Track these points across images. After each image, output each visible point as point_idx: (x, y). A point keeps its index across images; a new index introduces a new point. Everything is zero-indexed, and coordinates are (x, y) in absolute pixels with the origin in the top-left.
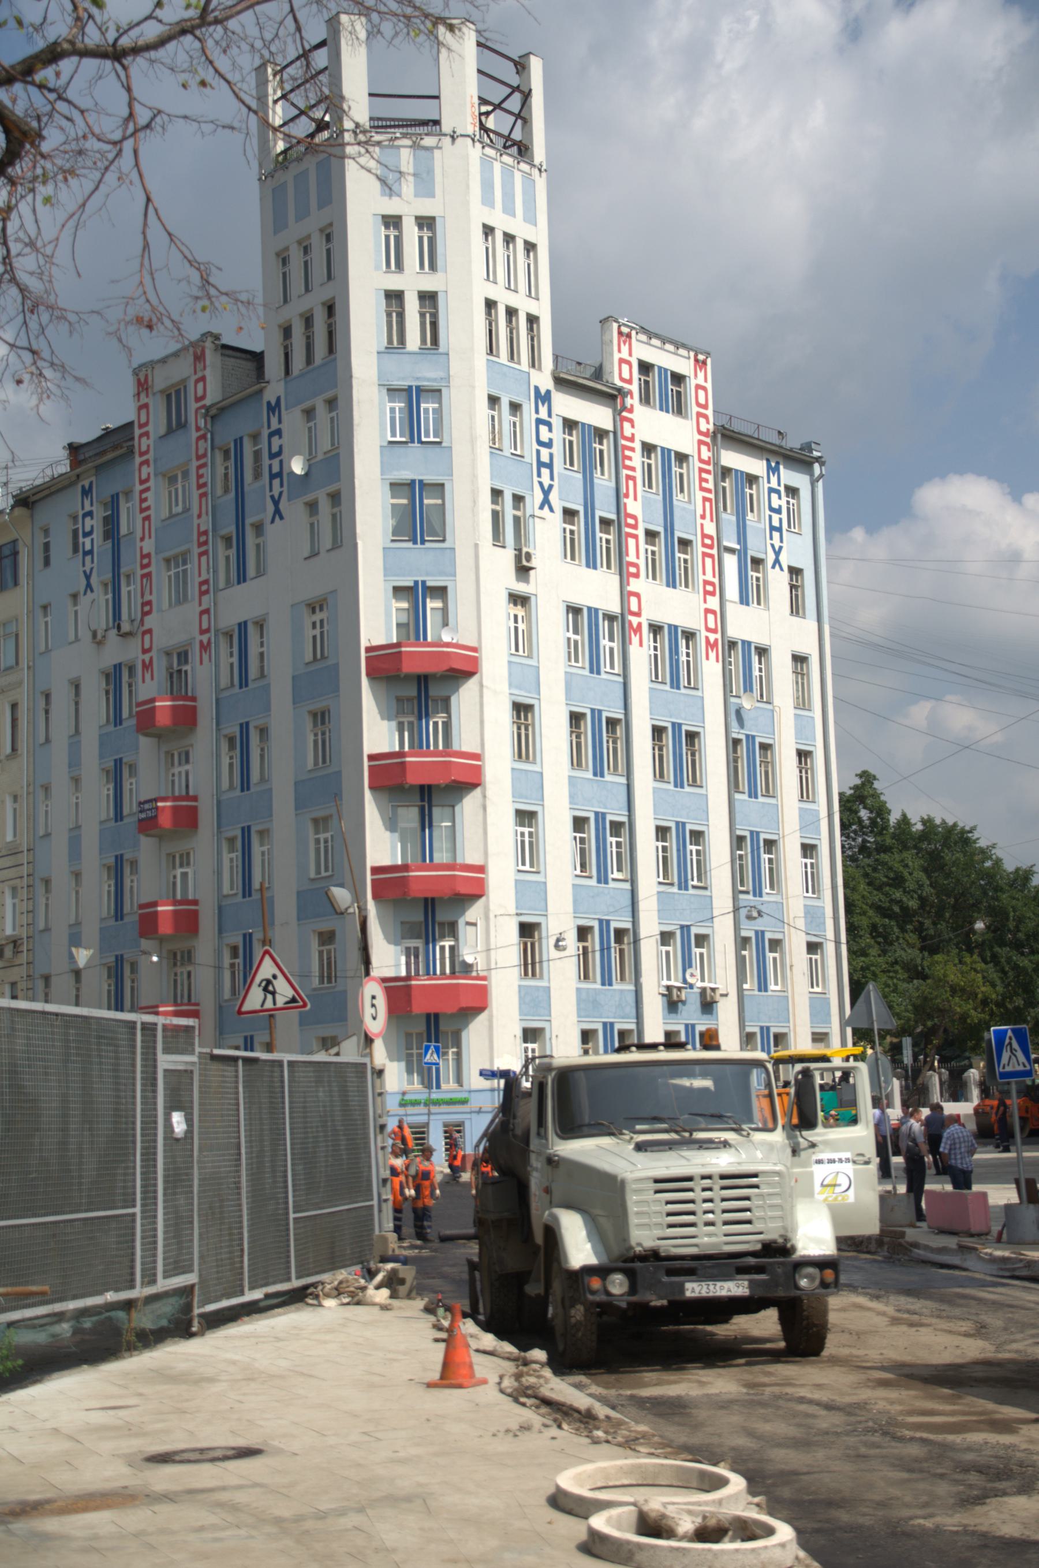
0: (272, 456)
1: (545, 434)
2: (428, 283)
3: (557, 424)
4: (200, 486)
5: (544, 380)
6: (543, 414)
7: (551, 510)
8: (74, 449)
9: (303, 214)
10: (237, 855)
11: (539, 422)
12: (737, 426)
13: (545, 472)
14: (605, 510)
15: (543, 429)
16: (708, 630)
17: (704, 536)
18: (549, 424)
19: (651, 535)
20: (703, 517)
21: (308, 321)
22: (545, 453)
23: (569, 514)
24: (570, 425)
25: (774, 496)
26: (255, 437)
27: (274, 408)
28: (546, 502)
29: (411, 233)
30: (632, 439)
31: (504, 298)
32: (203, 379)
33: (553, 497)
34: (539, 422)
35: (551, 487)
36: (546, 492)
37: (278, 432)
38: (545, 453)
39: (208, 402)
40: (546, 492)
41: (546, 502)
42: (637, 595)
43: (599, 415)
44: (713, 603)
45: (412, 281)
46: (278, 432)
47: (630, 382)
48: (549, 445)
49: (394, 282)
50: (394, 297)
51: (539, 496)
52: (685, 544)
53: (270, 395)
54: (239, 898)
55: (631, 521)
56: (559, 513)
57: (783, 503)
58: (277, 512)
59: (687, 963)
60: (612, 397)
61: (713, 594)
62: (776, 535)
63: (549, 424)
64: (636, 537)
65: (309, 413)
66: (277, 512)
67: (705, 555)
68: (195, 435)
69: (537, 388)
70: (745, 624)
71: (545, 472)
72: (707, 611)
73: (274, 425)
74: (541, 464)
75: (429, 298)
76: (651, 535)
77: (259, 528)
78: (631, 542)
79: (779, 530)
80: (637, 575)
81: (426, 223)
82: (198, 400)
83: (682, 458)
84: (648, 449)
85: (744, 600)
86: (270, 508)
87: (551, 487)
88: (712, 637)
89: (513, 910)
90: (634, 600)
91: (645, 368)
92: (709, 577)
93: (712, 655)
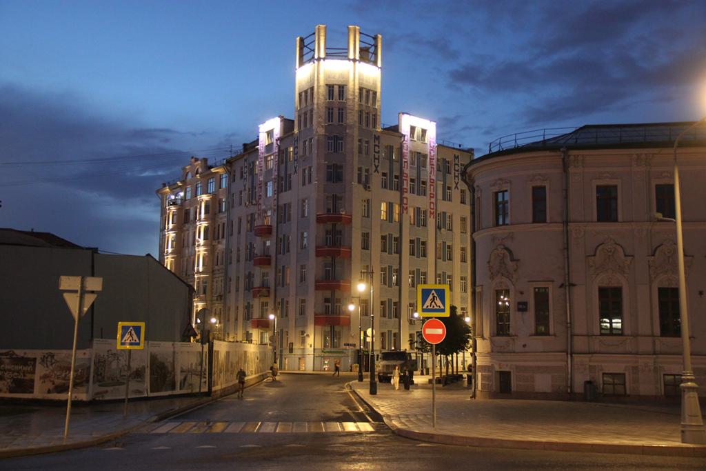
6: (377, 143)
7: (378, 172)
8: (245, 145)
14: (396, 173)
16: (431, 209)
17: (431, 179)
19: (412, 180)
20: (431, 173)
22: (377, 155)
25: (456, 166)
28: (376, 170)
34: (375, 146)
35: (378, 166)
36: (377, 167)
38: (377, 155)
40: (377, 167)
41: (376, 170)
42: (407, 198)
44: (433, 200)
51: (374, 169)
52: (424, 183)
55: (405, 175)
56: (380, 174)
61: (433, 197)
62: (456, 178)
63: (379, 147)
67: (430, 185)
69: (375, 136)
70: (443, 206)
71: (377, 161)
72: (431, 203)
74: (375, 159)
76: (412, 180)
78: (405, 182)
80: (406, 192)
85: (444, 199)
87: (378, 166)
88: (432, 211)
90: (405, 200)
92: (432, 192)
93: (432, 217)
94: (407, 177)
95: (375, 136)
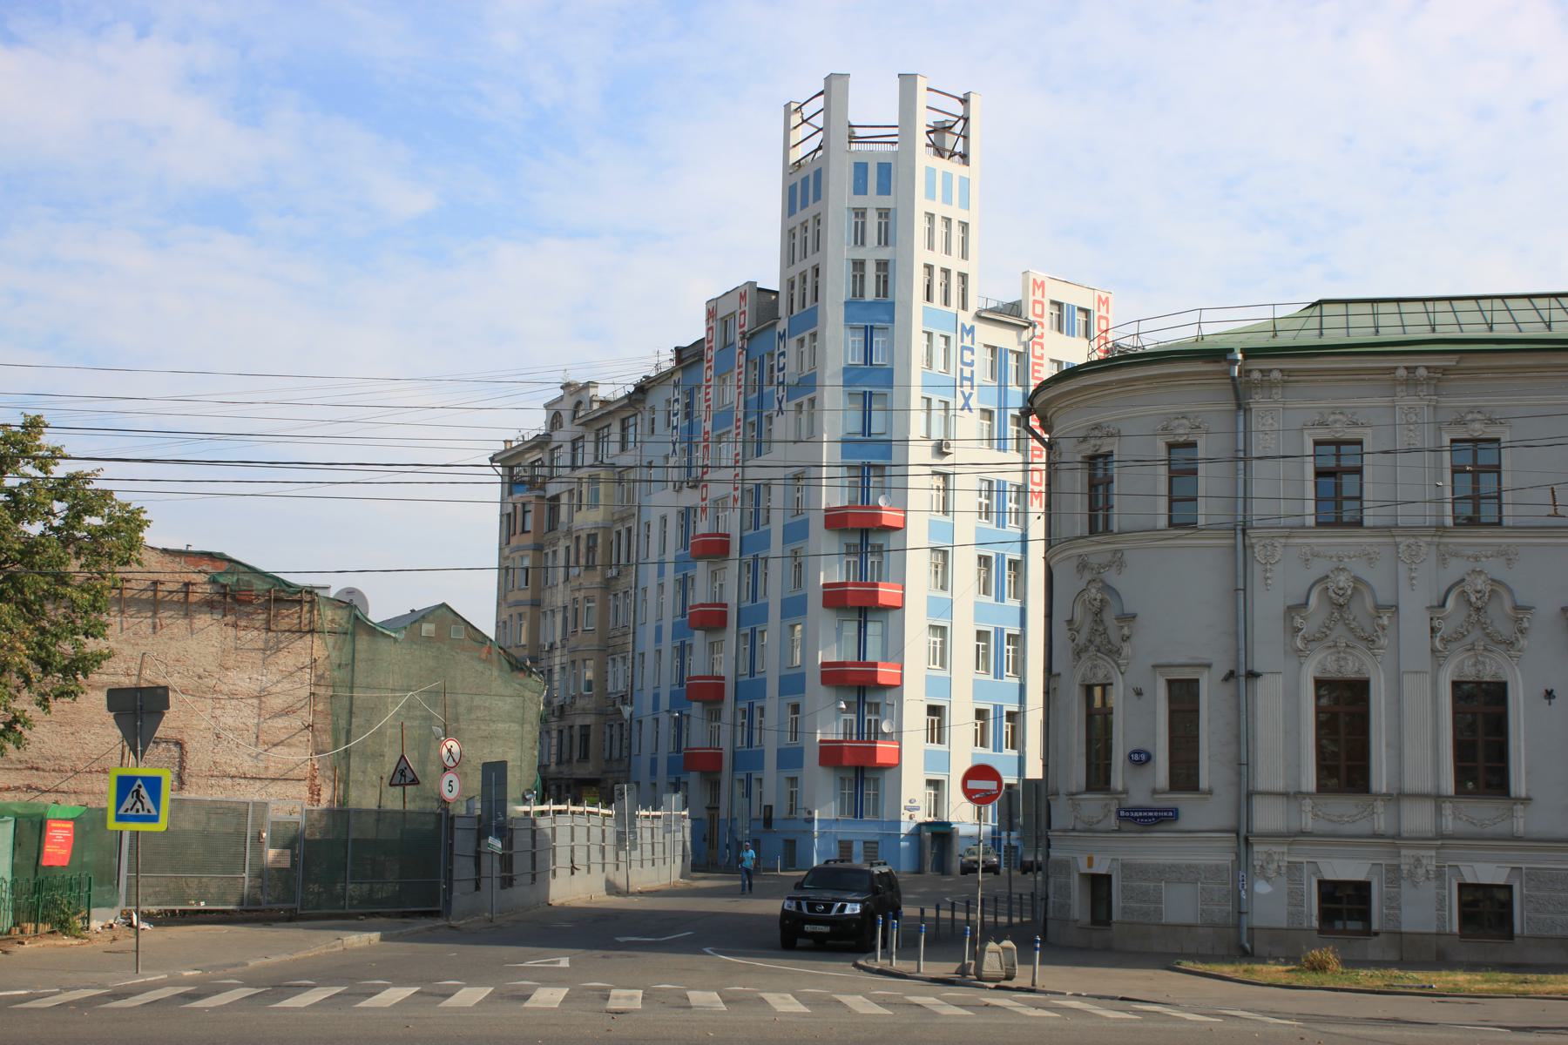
0: (780, 370)
1: (968, 357)
2: (884, 254)
5: (966, 318)
11: (963, 348)
15: (967, 354)
23: (987, 414)
27: (782, 337)
33: (973, 403)
34: (963, 348)
36: (967, 399)
37: (783, 354)
40: (967, 399)
46: (783, 354)
49: (859, 254)
50: (859, 265)
56: (977, 413)
77: (770, 418)
81: (884, 213)
86: (777, 406)
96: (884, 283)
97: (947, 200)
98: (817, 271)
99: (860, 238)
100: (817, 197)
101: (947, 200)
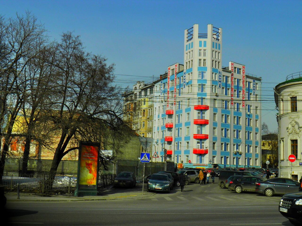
0: (184, 80)
1: (220, 77)
2: (205, 58)
3: (222, 76)
4: (175, 83)
6: (220, 75)
9: (189, 49)
10: (178, 131)
12: (250, 75)
13: (220, 82)
15: (220, 77)
18: (221, 76)
21: (189, 62)
24: (224, 76)
26: (182, 77)
27: (185, 73)
29: (202, 52)
30: (233, 78)
31: (215, 60)
32: (176, 69)
34: (219, 76)
36: (220, 85)
37: (185, 77)
39: (177, 72)
40: (220, 85)
43: (229, 75)
45: (202, 58)
47: (233, 70)
48: (221, 79)
50: (200, 60)
53: (184, 72)
54: (177, 137)
57: (255, 86)
58: (184, 87)
59: (237, 148)
60: (230, 72)
63: (221, 76)
64: (233, 91)
65: (189, 74)
66: (184, 87)
68: (175, 76)
69: (219, 71)
73: (185, 76)
74: (219, 81)
75: (204, 60)
77: (182, 88)
79: (255, 89)
81: (205, 50)
82: (176, 71)
83: (240, 80)
84: (235, 79)
86: (184, 87)
89: (212, 141)
91: (235, 68)
94: (233, 89)
95: (219, 71)
96: (204, 64)
97: (216, 48)
98: (192, 61)
99: (200, 54)
100: (192, 47)
101: (216, 48)
